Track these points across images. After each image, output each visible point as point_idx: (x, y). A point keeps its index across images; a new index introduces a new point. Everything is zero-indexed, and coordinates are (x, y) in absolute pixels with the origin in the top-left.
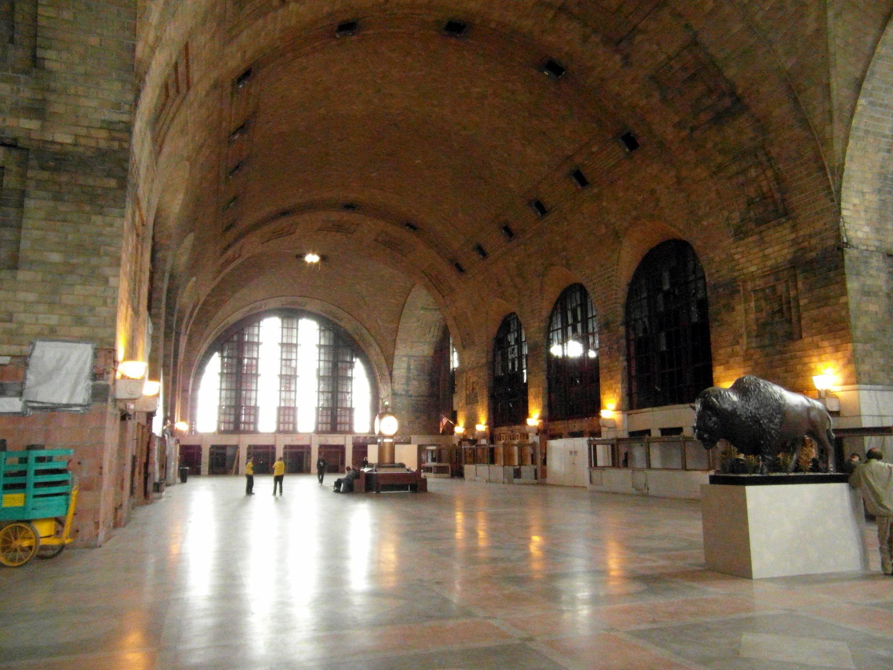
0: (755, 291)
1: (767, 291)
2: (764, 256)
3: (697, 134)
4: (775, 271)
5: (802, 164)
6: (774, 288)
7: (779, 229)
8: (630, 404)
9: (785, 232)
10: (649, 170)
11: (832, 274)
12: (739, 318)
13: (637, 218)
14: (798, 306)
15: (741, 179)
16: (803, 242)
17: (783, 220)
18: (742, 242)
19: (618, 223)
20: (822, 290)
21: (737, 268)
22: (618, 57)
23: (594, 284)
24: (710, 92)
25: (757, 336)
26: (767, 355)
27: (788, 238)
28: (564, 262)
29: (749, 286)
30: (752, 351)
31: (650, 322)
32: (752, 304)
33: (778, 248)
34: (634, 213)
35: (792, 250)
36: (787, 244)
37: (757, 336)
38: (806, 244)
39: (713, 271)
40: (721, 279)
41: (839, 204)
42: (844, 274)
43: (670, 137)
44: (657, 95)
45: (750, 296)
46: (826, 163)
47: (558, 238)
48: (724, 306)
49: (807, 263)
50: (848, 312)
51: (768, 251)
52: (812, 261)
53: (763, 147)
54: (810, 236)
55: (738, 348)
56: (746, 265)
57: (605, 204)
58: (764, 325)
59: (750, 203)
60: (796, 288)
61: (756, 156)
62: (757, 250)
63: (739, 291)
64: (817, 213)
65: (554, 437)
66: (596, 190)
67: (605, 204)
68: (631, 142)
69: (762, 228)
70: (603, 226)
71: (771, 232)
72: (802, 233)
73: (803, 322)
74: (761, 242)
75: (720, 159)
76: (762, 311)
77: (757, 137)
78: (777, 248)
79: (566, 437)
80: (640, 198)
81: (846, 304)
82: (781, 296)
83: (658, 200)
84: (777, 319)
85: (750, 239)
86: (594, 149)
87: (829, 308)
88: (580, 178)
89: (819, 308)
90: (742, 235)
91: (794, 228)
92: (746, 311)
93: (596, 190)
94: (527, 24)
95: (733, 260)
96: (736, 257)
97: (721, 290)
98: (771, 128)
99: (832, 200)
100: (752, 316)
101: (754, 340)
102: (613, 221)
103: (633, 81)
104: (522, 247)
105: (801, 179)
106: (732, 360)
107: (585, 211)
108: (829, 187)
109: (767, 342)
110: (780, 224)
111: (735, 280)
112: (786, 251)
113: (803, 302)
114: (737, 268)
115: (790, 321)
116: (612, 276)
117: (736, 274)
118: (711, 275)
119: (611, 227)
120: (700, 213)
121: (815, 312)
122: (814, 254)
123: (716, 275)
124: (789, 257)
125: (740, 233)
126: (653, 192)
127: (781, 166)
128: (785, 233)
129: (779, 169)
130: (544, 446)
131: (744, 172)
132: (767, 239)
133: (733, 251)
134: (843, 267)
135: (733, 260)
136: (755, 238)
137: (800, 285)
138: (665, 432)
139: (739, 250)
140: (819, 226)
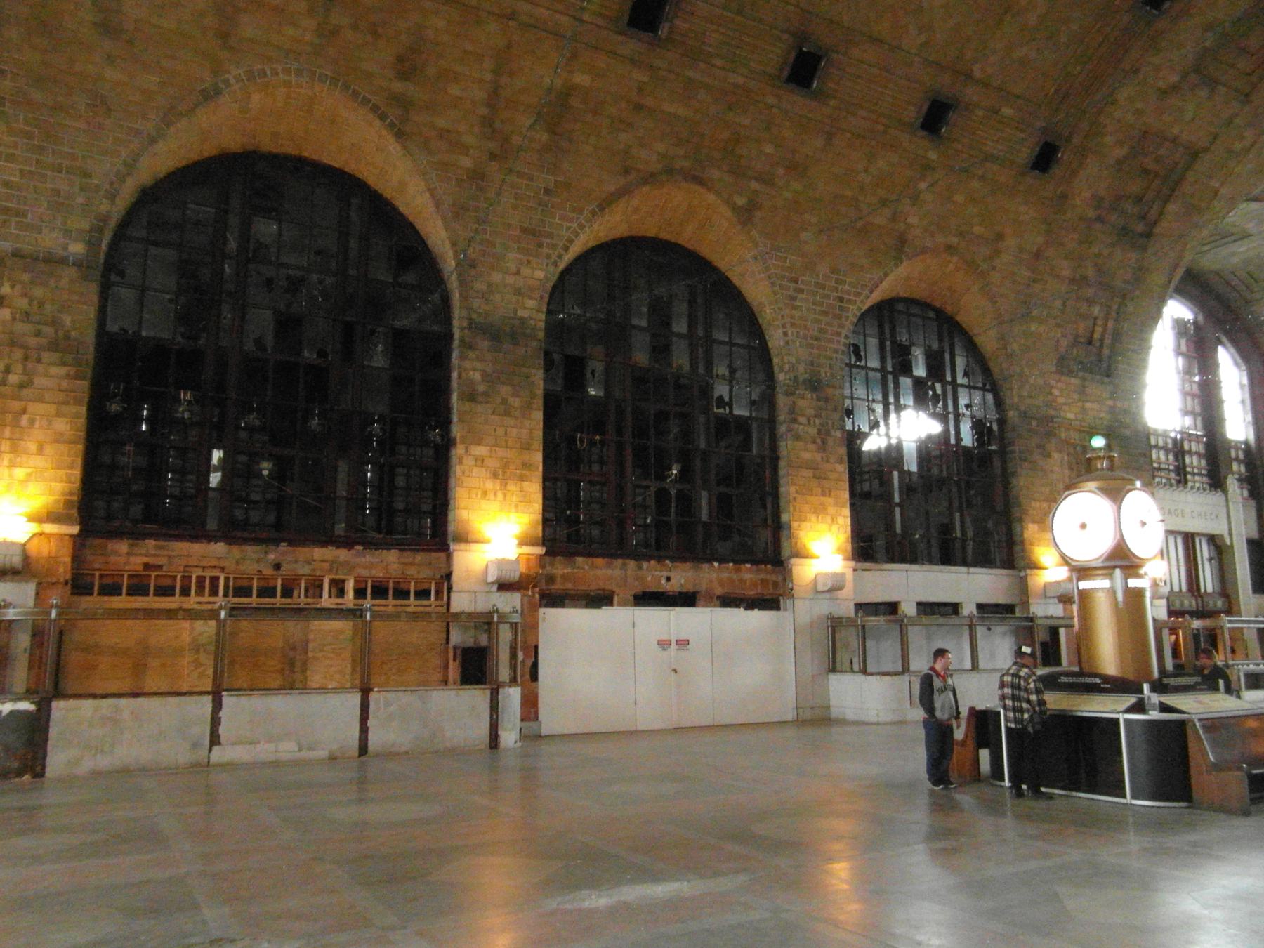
3: (1098, 226)
8: (865, 549)
10: (1022, 209)
13: (950, 249)
17: (1106, 380)
19: (918, 232)
22: (1174, 78)
23: (801, 291)
24: (1139, 200)
34: (954, 240)
35: (1108, 417)
43: (1078, 202)
44: (1121, 152)
47: (769, 149)
51: (1088, 405)
53: (1124, 297)
57: (923, 185)
65: (555, 600)
66: (933, 155)
68: (1045, 159)
70: (887, 212)
75: (1090, 272)
79: (623, 604)
80: (977, 230)
83: (997, 253)
85: (1073, 380)
86: (1007, 111)
88: (935, 117)
93: (933, 155)
96: (1056, 392)
103: (1138, 112)
104: (640, 76)
107: (881, 163)
116: (849, 301)
117: (1052, 412)
118: (1020, 396)
119: (902, 227)
120: (1035, 313)
123: (1028, 401)
126: (1000, 237)
130: (531, 627)
131: (1091, 302)
132: (1088, 390)
135: (1051, 394)
138: (926, 608)
139: (1059, 385)
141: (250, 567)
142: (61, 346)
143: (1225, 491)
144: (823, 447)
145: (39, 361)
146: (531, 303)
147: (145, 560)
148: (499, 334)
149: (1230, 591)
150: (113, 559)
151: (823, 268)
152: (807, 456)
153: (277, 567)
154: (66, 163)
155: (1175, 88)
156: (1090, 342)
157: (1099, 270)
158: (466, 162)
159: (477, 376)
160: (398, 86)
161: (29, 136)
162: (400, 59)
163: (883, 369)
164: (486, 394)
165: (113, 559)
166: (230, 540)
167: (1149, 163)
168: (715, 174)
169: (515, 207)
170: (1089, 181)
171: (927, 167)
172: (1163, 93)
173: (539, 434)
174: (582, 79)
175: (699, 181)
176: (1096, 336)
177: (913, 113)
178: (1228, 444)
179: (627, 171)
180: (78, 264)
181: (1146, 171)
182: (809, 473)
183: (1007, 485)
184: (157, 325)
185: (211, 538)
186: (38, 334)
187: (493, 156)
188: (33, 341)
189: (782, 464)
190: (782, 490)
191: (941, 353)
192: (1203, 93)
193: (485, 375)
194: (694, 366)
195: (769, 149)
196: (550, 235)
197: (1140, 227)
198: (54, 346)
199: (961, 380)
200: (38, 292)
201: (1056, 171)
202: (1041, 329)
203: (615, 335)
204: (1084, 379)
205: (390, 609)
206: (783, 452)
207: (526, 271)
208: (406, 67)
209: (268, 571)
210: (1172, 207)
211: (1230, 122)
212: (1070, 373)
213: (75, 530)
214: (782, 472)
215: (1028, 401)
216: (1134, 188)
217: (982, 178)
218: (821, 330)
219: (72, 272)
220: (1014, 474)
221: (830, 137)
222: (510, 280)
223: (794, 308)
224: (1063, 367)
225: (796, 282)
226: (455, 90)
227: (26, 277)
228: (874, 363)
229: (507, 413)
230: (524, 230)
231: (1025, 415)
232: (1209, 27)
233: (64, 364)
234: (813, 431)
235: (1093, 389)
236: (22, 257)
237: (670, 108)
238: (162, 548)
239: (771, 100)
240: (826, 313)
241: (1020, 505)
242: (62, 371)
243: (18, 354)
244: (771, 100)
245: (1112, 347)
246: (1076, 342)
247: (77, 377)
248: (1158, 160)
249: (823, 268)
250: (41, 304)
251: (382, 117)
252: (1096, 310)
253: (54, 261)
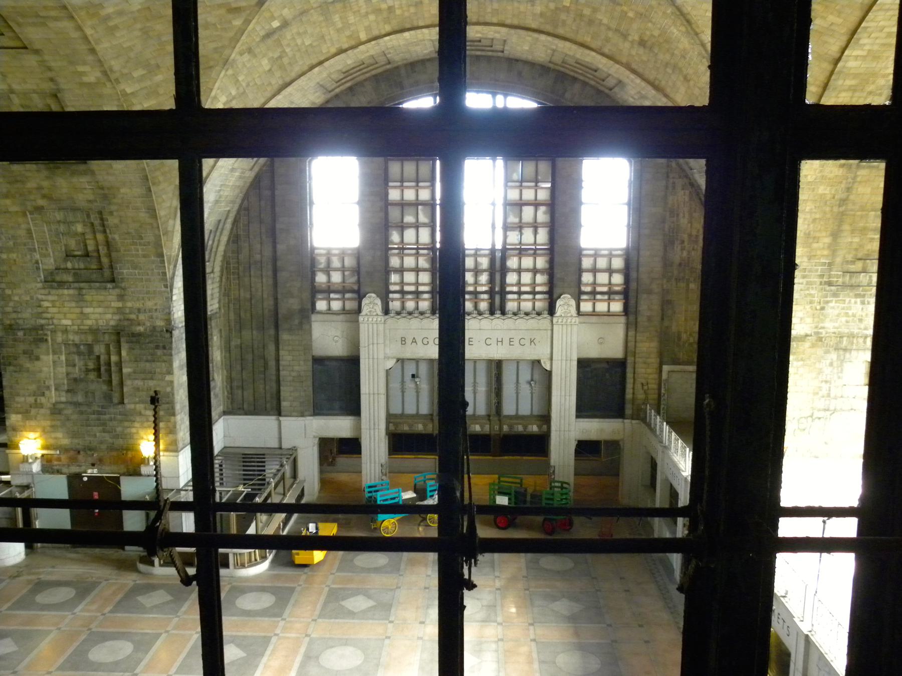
0: (66, 345)
1: (82, 347)
2: (82, 313)
4: (94, 331)
5: (140, 244)
6: (90, 347)
7: (103, 292)
9: (110, 298)
11: (159, 352)
12: (45, 369)
14: (121, 370)
15: (62, 228)
16: (130, 313)
17: (109, 285)
18: (53, 292)
20: (148, 364)
21: (45, 315)
25: (68, 391)
26: (81, 413)
27: (113, 304)
29: (60, 338)
30: (62, 406)
32: (63, 358)
33: (100, 310)
35: (117, 317)
36: (111, 310)
37: (68, 391)
38: (133, 316)
39: (9, 309)
40: (21, 322)
41: (171, 291)
42: (171, 355)
45: (61, 348)
46: (165, 252)
48: (25, 352)
49: (133, 335)
50: (172, 389)
51: (87, 310)
52: (140, 334)
54: (139, 310)
55: (43, 400)
56: (57, 316)
58: (75, 380)
59: (69, 255)
60: (120, 354)
61: (88, 216)
62: (73, 304)
63: (46, 340)
64: (148, 292)
69: (82, 285)
71: (93, 292)
72: (129, 304)
73: (125, 390)
74: (80, 298)
76: (74, 366)
77: (96, 201)
78: (100, 310)
81: (172, 382)
82: (98, 357)
84: (92, 376)
85: (66, 292)
87: (155, 382)
89: (144, 379)
90: (55, 284)
91: (121, 297)
92: (54, 362)
95: (40, 306)
96: (46, 304)
97: (20, 334)
98: (115, 201)
99: (166, 286)
100: (62, 370)
101: (64, 394)
105: (137, 256)
106: (33, 412)
108: (164, 274)
109: (80, 398)
110: (106, 288)
111: (42, 327)
112: (109, 316)
113: (126, 370)
114: (45, 315)
115: (110, 382)
117: (43, 322)
121: (139, 383)
122: (141, 329)
123: (14, 316)
124: (112, 323)
125: (52, 281)
127: (117, 237)
128: (110, 296)
129: (114, 239)
131: (68, 223)
133: (40, 297)
134: (171, 348)
135: (40, 306)
136: (71, 292)
137: (124, 353)
139: (50, 298)
140: (150, 304)
176: (90, 248)
202: (14, 256)
204: (81, 289)
215: (14, 316)
245: (109, 256)
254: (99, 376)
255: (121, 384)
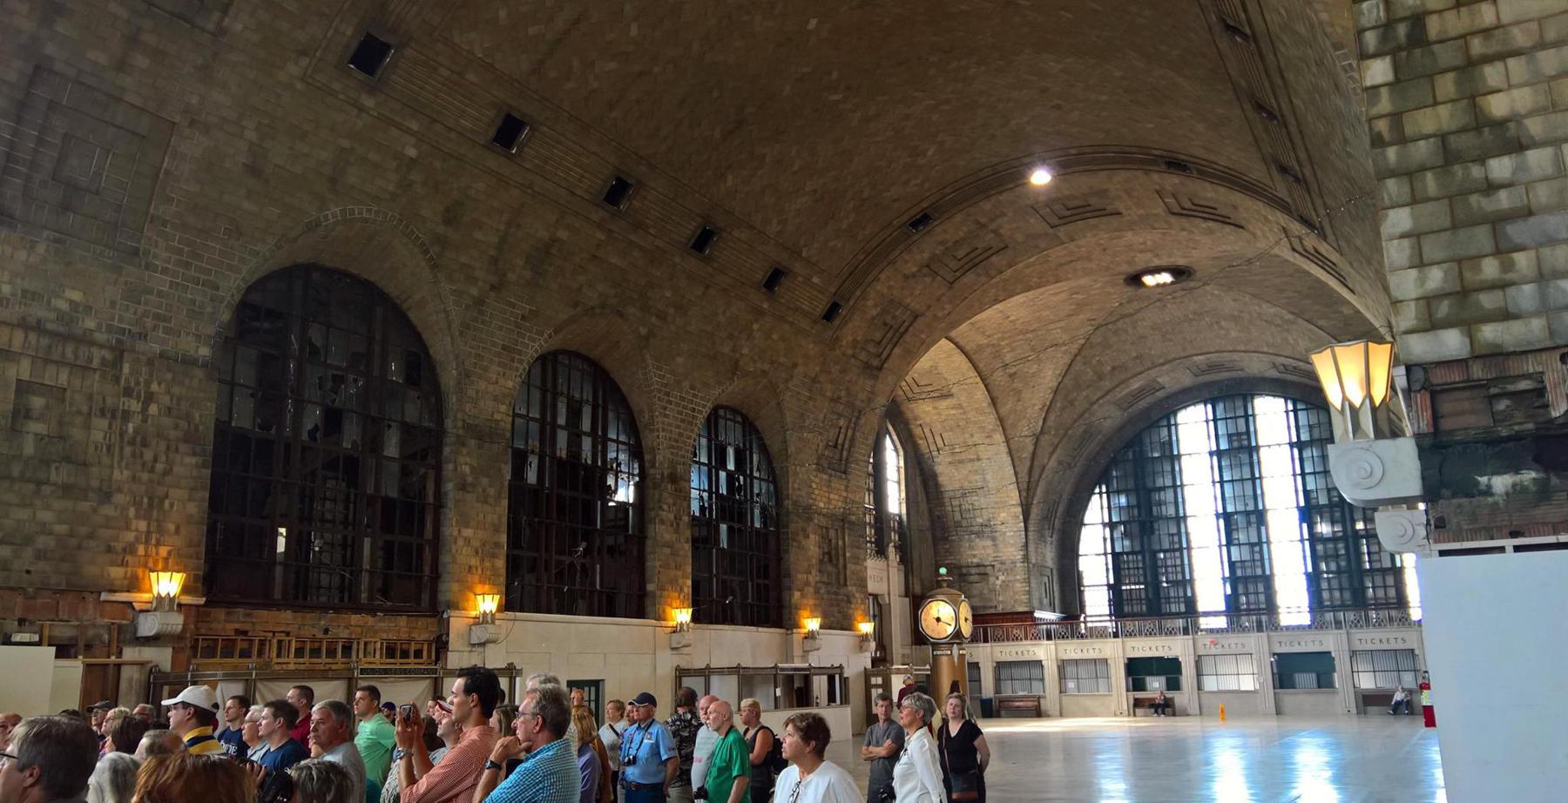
22: (914, 269)
28: (643, 331)
31: (710, 498)
34: (766, 367)
44: (874, 312)
47: (668, 294)
57: (756, 327)
66: (765, 306)
67: (756, 327)
68: (831, 313)
80: (782, 360)
83: (792, 377)
86: (815, 280)
88: (774, 278)
94: (987, 206)
102: (745, 351)
103: (890, 288)
104: (601, 236)
126: (795, 365)
131: (840, 415)
141: (307, 632)
142: (190, 438)
143: (887, 558)
144: (677, 531)
145: (177, 450)
146: (503, 408)
147: (237, 626)
148: (481, 433)
149: (886, 642)
150: (214, 626)
151: (686, 384)
152: (667, 537)
153: (326, 631)
154: (202, 277)
155: (914, 275)
156: (835, 447)
157: (848, 394)
158: (474, 292)
159: (467, 470)
160: (441, 229)
161: (179, 252)
162: (447, 210)
163: (709, 465)
164: (473, 485)
165: (214, 626)
166: (296, 608)
167: (888, 319)
168: (631, 310)
169: (501, 328)
170: (854, 328)
171: (759, 313)
172: (906, 277)
173: (505, 519)
174: (563, 234)
175: (621, 315)
177: (760, 276)
178: (888, 515)
179: (576, 305)
180: (205, 366)
181: (885, 324)
182: (668, 551)
183: (779, 560)
184: (244, 417)
185: (279, 606)
186: (176, 427)
187: (493, 288)
188: (173, 434)
189: (649, 543)
190: (649, 564)
191: (744, 450)
192: (928, 280)
193: (472, 467)
194: (594, 460)
195: (668, 294)
196: (520, 353)
197: (875, 363)
198: (187, 439)
199: (756, 474)
200: (176, 390)
201: (837, 322)
203: (547, 430)
205: (292, 667)
206: (650, 532)
207: (502, 381)
208: (451, 217)
209: (320, 635)
210: (897, 351)
211: (938, 300)
212: (823, 471)
213: (202, 601)
214: (648, 550)
216: (878, 336)
217: (791, 324)
218: (680, 435)
219: (199, 373)
220: (787, 551)
221: (708, 287)
222: (491, 388)
223: (666, 416)
224: (820, 468)
225: (668, 394)
226: (478, 235)
227: (169, 376)
228: (704, 459)
229: (485, 502)
230: (504, 348)
231: (795, 503)
232: (941, 243)
233: (194, 454)
234: (671, 516)
235: (836, 484)
236: (167, 358)
237: (614, 260)
238: (248, 615)
239: (677, 260)
240: (683, 421)
241: (789, 576)
242: (193, 460)
243: (163, 446)
244: (677, 260)
246: (827, 446)
247: (204, 466)
248: (894, 317)
249: (686, 384)
250: (179, 399)
251: (426, 252)
252: (842, 422)
253: (189, 362)
254: (830, 560)
255: (845, 567)
